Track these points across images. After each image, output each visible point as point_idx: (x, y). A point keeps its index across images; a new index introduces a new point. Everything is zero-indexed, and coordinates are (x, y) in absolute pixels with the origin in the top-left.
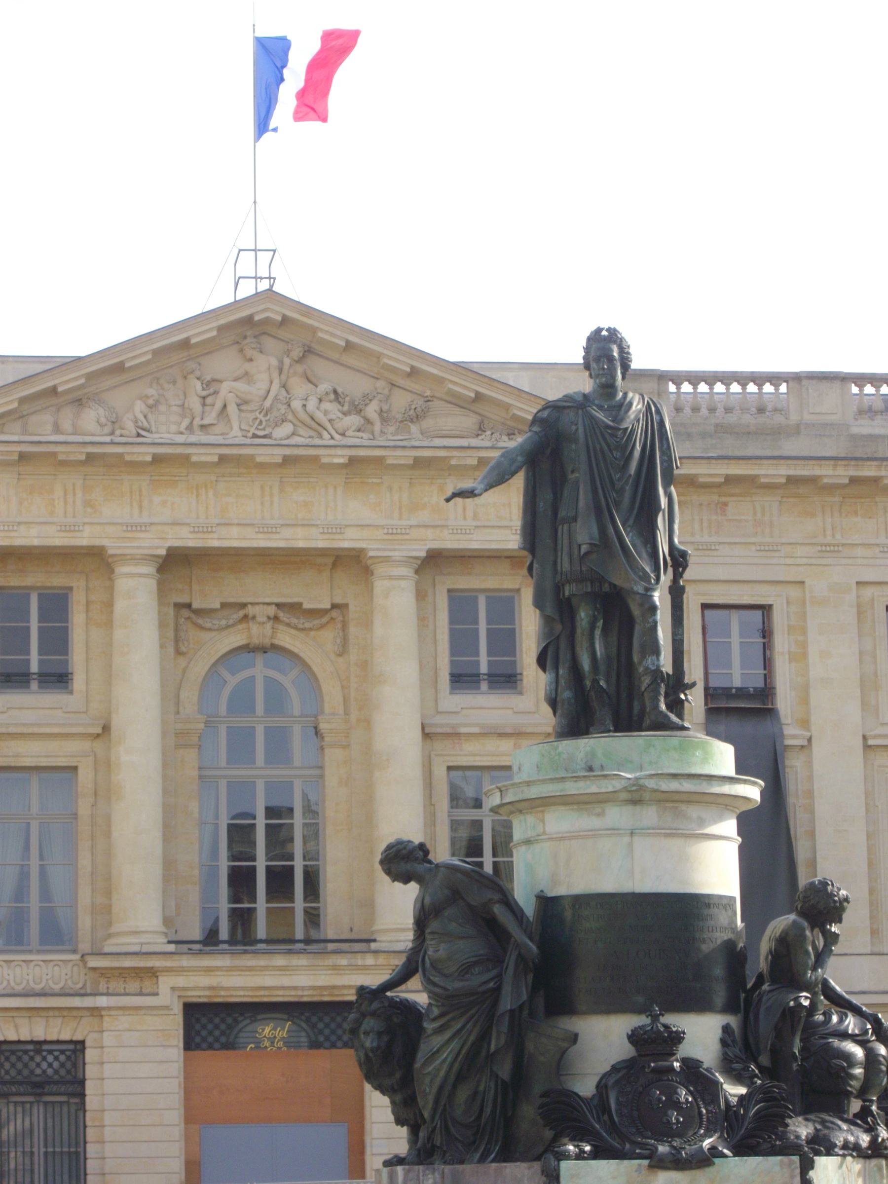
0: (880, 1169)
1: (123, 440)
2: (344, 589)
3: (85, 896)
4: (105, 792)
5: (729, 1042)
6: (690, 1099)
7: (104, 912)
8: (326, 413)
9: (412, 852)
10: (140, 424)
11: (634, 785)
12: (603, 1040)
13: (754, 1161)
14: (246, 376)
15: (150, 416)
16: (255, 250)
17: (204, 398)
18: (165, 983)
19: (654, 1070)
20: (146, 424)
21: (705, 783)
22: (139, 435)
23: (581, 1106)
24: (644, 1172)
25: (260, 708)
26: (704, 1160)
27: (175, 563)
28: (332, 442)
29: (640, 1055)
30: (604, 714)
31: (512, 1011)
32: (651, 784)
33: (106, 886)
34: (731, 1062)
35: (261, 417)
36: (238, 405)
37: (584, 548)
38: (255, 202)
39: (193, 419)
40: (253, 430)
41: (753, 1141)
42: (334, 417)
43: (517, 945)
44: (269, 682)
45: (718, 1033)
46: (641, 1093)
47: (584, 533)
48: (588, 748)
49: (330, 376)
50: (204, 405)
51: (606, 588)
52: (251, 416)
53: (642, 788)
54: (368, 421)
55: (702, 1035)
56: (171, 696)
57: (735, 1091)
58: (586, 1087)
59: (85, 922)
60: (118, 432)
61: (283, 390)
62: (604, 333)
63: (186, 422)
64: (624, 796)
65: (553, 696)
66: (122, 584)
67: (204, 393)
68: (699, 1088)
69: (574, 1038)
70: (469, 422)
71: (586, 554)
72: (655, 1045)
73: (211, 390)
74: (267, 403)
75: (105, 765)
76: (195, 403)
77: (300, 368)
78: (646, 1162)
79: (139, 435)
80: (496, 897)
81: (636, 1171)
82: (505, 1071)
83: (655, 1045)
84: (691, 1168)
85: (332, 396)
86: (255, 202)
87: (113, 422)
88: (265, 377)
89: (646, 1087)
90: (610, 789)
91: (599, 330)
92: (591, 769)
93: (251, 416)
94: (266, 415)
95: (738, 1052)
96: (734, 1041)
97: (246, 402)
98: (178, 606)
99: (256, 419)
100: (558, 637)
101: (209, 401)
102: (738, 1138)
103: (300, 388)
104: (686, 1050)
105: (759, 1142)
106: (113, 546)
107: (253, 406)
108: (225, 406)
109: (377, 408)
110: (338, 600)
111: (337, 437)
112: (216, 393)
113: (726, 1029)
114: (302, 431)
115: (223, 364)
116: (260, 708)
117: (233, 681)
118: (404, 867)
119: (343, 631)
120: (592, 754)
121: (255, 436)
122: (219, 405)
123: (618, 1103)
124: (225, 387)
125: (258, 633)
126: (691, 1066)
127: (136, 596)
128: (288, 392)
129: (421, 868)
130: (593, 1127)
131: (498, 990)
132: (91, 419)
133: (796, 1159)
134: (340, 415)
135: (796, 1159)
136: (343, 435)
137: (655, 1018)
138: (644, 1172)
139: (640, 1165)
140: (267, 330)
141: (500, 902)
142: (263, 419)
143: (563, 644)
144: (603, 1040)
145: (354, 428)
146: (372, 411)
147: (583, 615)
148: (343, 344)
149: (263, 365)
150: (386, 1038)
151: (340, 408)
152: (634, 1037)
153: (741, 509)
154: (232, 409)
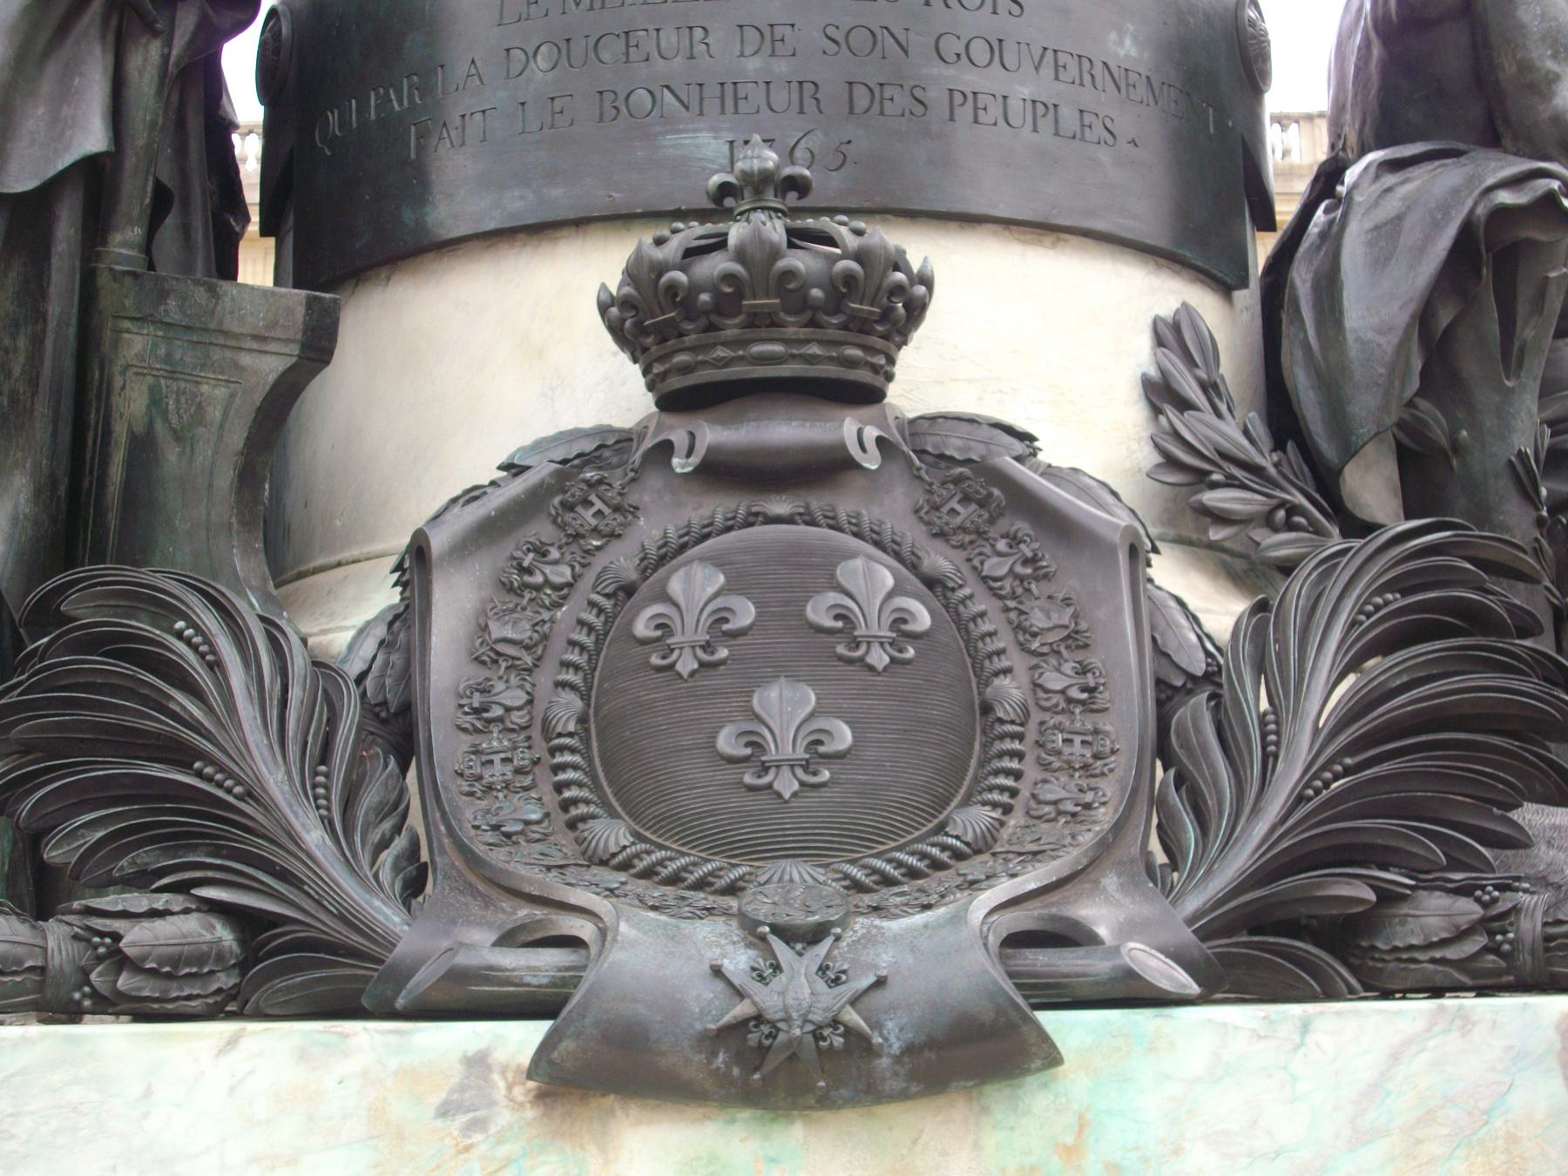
5: (1194, 393)
6: (923, 619)
13: (1355, 1035)
19: (720, 471)
23: (216, 666)
24: (504, 1117)
34: (1200, 479)
41: (1352, 889)
45: (1140, 356)
46: (629, 590)
68: (996, 567)
78: (521, 1039)
81: (445, 1111)
84: (871, 1093)
89: (662, 560)
96: (1211, 388)
102: (1240, 860)
104: (931, 375)
105: (1388, 897)
113: (1172, 335)
123: (487, 655)
126: (981, 485)
138: (512, 1108)
139: (478, 1063)
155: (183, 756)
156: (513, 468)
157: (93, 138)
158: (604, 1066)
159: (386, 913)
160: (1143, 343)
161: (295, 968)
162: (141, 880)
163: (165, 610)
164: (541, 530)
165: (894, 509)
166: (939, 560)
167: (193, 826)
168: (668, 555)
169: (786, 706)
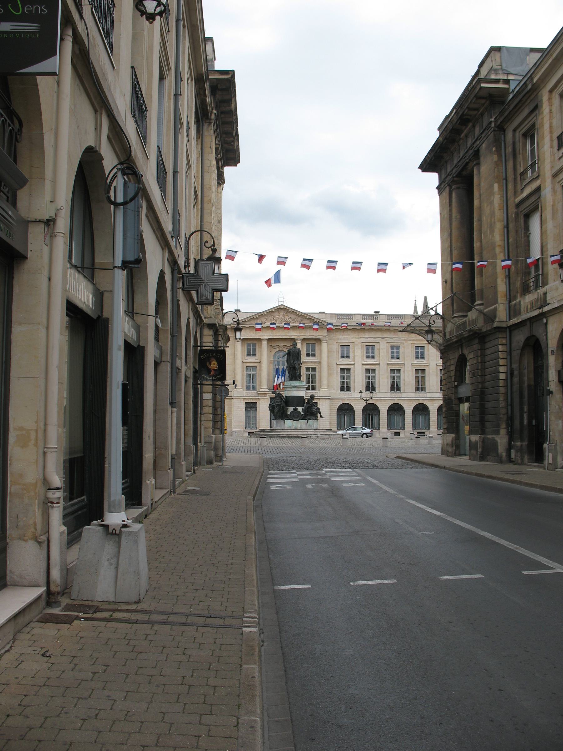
3: (258, 383)
4: (260, 370)
7: (260, 386)
12: (291, 409)
18: (267, 395)
27: (270, 340)
33: (261, 382)
49: (290, 316)
55: (300, 409)
56: (269, 357)
57: (302, 413)
58: (289, 413)
59: (258, 387)
66: (263, 343)
72: (295, 410)
75: (261, 367)
83: (295, 410)
103: (286, 317)
106: (261, 338)
115: (276, 314)
117: (277, 355)
125: (281, 349)
127: (265, 344)
140: (282, 309)
144: (291, 409)
149: (282, 313)
153: (346, 332)
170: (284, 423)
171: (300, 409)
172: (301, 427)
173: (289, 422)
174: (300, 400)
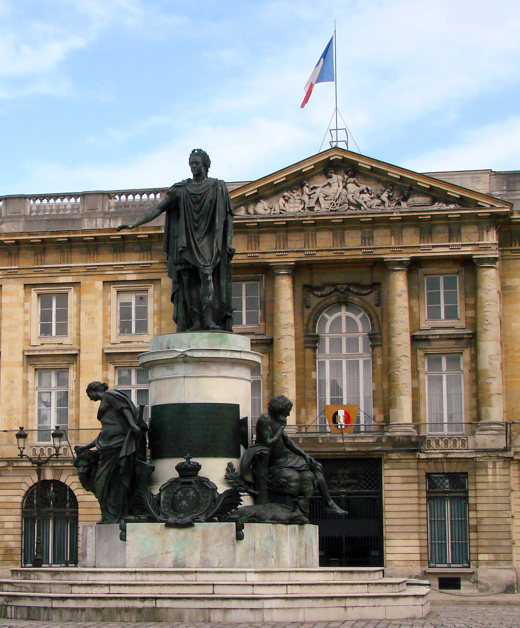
0: (295, 529)
1: (274, 216)
2: (377, 276)
5: (230, 471)
8: (363, 199)
9: (97, 387)
10: (281, 208)
11: (182, 355)
14: (329, 184)
15: (286, 205)
16: (337, 129)
17: (309, 195)
19: (183, 483)
20: (284, 208)
21: (216, 353)
22: (281, 213)
25: (344, 329)
26: (189, 525)
28: (365, 212)
29: (181, 476)
30: (197, 323)
31: (128, 457)
32: (189, 354)
35: (334, 202)
36: (324, 198)
37: (181, 249)
38: (336, 108)
39: (305, 204)
40: (331, 209)
42: (366, 200)
43: (133, 428)
44: (347, 318)
47: (182, 241)
48: (168, 339)
50: (310, 198)
51: (191, 267)
52: (330, 202)
53: (186, 356)
54: (383, 203)
60: (272, 213)
61: (344, 190)
62: (196, 152)
63: (302, 206)
64: (181, 360)
65: (176, 316)
67: (311, 193)
69: (153, 468)
70: (428, 200)
71: (181, 251)
73: (313, 192)
74: (337, 196)
76: (306, 198)
77: (352, 180)
78: (164, 524)
79: (281, 213)
80: (125, 406)
82: (126, 483)
83: (189, 472)
85: (366, 191)
86: (336, 108)
87: (271, 208)
88: (336, 184)
90: (172, 357)
91: (194, 150)
92: (169, 348)
93: (330, 202)
94: (336, 201)
95: (230, 475)
97: (326, 196)
98: (305, 286)
99: (331, 204)
100: (178, 290)
101: (312, 196)
107: (330, 198)
108: (318, 198)
109: (387, 196)
110: (375, 281)
111: (368, 209)
112: (315, 193)
113: (230, 465)
114: (352, 207)
116: (344, 329)
118: (94, 394)
119: (379, 295)
120: (169, 342)
121: (331, 211)
122: (315, 199)
123: (165, 498)
124: (318, 191)
128: (347, 190)
129: (101, 394)
130: (149, 508)
131: (121, 448)
132: (262, 208)
133: (234, 524)
134: (369, 199)
135: (234, 524)
136: (371, 208)
137: (188, 459)
140: (338, 164)
141: (127, 408)
142: (335, 203)
143: (180, 292)
145: (375, 205)
146: (384, 197)
147: (185, 278)
148: (370, 168)
149: (337, 179)
150: (86, 469)
151: (370, 196)
152: (178, 468)
154: (321, 200)
155: (144, 505)
156: (168, 482)
157: (134, 450)
158: (169, 525)
159: (157, 516)
160: (227, 465)
161: (152, 519)
162: (141, 514)
163: (142, 494)
164: (169, 488)
165: (196, 486)
166: (198, 491)
167: (144, 510)
168: (177, 491)
169: (184, 502)
170: (123, 538)
171: (215, 470)
172: (204, 562)
173: (145, 539)
174: (217, 427)
